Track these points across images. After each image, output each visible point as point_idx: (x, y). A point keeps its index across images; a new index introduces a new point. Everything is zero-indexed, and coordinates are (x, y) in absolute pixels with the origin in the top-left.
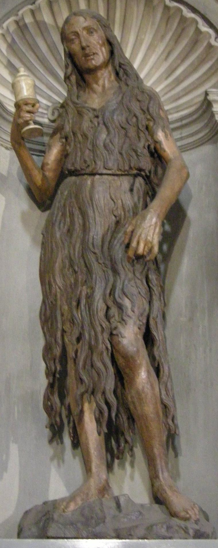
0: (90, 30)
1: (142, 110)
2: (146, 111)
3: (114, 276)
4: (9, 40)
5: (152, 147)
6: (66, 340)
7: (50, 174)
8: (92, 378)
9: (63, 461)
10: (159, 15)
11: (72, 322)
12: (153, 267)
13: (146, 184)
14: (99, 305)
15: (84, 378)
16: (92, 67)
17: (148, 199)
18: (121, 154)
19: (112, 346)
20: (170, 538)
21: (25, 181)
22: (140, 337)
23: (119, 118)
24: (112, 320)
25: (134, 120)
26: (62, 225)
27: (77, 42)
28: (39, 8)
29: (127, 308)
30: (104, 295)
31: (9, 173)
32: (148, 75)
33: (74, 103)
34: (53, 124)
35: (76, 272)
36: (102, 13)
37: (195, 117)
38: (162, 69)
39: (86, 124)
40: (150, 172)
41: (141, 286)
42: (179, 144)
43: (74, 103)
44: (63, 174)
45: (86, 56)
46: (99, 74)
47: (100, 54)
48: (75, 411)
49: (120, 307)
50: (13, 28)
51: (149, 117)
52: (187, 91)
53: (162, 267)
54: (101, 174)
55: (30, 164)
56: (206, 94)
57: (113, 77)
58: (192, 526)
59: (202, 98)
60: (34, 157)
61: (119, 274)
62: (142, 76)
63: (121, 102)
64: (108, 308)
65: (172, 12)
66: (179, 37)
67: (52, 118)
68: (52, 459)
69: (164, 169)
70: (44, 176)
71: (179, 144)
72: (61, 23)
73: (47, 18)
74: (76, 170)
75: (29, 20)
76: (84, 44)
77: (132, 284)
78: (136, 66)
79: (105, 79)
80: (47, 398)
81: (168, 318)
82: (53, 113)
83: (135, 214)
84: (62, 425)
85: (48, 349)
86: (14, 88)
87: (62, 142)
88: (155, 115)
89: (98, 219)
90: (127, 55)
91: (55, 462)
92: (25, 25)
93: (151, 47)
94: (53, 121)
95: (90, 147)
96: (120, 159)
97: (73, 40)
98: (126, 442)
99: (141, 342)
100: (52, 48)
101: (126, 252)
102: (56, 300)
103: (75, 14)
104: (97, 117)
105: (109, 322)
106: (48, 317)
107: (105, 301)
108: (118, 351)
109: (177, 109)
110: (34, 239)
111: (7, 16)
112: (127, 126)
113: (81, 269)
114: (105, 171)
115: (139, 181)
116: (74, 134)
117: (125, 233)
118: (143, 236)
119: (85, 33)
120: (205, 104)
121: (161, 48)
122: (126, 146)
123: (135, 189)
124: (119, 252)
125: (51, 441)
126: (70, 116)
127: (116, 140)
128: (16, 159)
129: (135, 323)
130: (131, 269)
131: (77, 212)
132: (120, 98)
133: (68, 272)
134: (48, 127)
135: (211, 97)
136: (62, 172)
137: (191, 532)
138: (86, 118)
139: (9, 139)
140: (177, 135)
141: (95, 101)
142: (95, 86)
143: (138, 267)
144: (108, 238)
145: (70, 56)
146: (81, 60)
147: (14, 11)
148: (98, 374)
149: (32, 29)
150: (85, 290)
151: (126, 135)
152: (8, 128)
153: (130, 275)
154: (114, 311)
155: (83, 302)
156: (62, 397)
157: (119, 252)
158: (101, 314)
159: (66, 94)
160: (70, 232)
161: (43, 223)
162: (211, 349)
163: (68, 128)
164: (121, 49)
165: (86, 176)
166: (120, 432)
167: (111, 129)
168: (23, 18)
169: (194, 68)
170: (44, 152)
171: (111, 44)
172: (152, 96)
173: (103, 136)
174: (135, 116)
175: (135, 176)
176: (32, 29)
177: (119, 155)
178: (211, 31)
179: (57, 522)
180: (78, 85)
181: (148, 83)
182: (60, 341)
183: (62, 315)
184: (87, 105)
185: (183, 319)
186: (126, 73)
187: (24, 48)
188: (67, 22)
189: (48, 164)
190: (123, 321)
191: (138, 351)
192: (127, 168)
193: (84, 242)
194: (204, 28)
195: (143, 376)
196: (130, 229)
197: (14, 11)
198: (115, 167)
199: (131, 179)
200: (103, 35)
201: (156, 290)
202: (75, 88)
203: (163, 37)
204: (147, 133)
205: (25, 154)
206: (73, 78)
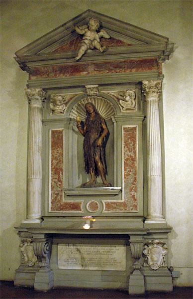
39: (90, 123)
44: (87, 132)
84: (88, 171)
85: (85, 160)
106: (85, 155)
113: (89, 148)
121: (104, 107)
145: (87, 111)
166: (97, 173)
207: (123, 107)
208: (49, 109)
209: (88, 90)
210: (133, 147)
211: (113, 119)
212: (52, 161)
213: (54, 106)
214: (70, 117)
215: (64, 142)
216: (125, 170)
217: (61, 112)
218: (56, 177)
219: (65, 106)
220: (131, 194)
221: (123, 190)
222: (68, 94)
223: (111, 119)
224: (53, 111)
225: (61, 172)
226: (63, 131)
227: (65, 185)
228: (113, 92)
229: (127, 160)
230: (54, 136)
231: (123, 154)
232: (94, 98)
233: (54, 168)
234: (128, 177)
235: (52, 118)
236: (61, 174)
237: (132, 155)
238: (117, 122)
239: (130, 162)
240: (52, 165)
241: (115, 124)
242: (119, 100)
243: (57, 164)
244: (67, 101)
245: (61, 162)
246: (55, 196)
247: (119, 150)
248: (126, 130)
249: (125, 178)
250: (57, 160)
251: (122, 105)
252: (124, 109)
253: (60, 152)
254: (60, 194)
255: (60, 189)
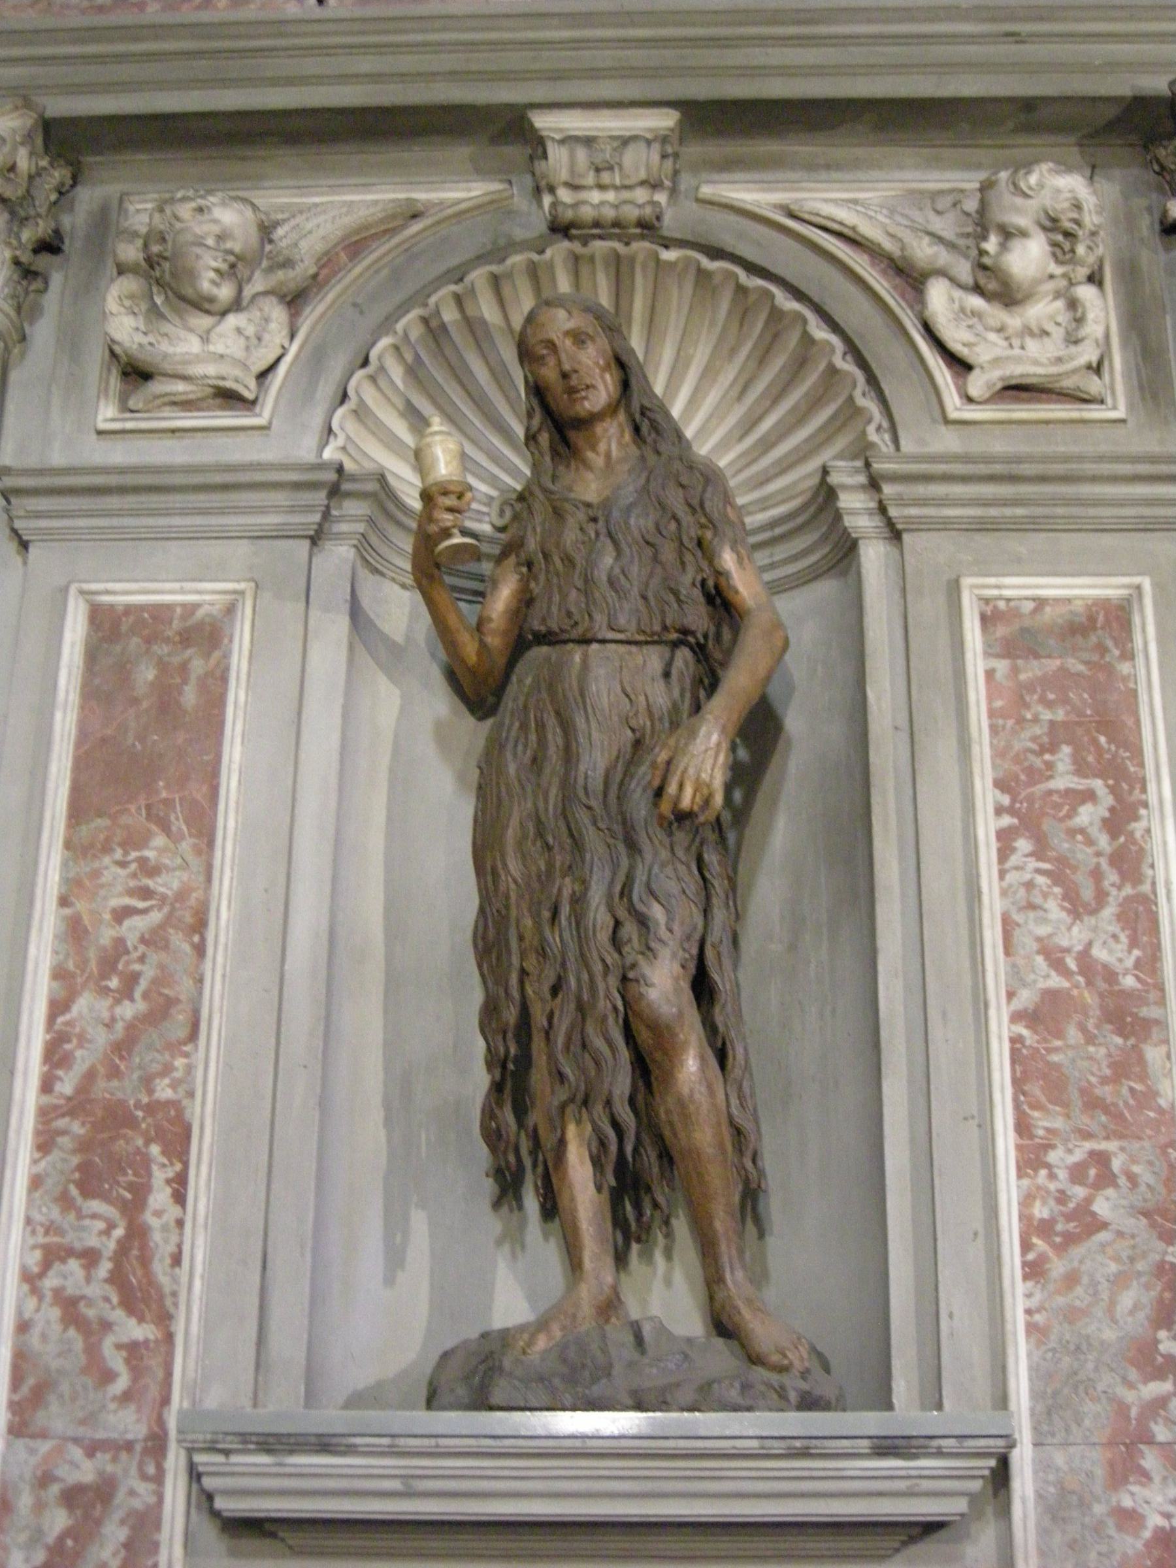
0: (579, 338)
1: (690, 505)
2: (697, 508)
3: (631, 856)
4: (409, 357)
5: (711, 583)
6: (529, 991)
7: (494, 641)
8: (583, 1071)
9: (523, 1246)
10: (725, 305)
11: (542, 952)
12: (712, 837)
13: (698, 661)
14: (599, 916)
15: (568, 1070)
16: (583, 414)
17: (702, 694)
18: (644, 598)
19: (626, 1004)
20: (749, 1409)
21: (442, 655)
22: (685, 986)
23: (641, 522)
24: (626, 949)
25: (673, 526)
26: (520, 748)
27: (551, 361)
28: (472, 291)
29: (657, 924)
30: (609, 896)
31: (408, 638)
32: (703, 431)
33: (545, 490)
34: (502, 536)
35: (549, 848)
36: (605, 300)
37: (800, 520)
38: (731, 420)
39: (571, 536)
40: (706, 636)
41: (687, 878)
42: (767, 577)
43: (545, 490)
44: (524, 639)
45: (572, 391)
46: (599, 429)
47: (601, 387)
48: (548, 1140)
49: (643, 922)
50: (416, 332)
51: (703, 520)
52: (784, 466)
53: (731, 837)
54: (603, 641)
55: (452, 620)
56: (825, 471)
57: (628, 436)
58: (794, 1385)
59: (815, 480)
60: (462, 605)
61: (640, 852)
62: (689, 433)
63: (645, 490)
64: (618, 924)
65: (752, 298)
66: (768, 350)
67: (500, 523)
68: (499, 1243)
69: (736, 631)
70: (483, 644)
71: (767, 577)
72: (517, 322)
73: (488, 310)
74: (550, 633)
75: (450, 315)
76: (567, 367)
77: (667, 876)
78: (676, 412)
79: (612, 440)
80: (489, 1114)
81: (743, 943)
82: (502, 513)
83: (675, 725)
84: (519, 1171)
85: (490, 1010)
86: (419, 460)
87: (521, 574)
88: (716, 516)
89: (595, 735)
90: (658, 389)
91: (506, 1248)
92: (443, 327)
93: (709, 374)
94: (502, 529)
95: (579, 583)
96: (642, 608)
97: (543, 357)
98: (656, 1205)
99: (688, 995)
100: (499, 374)
101: (656, 805)
102: (507, 907)
103: (548, 303)
104: (594, 520)
105: (620, 953)
106: (491, 943)
107: (611, 910)
108: (638, 1015)
109: (764, 504)
110: (461, 777)
111: (403, 308)
112: (657, 540)
114: (611, 635)
115: (684, 656)
116: (546, 556)
117: (654, 765)
118: (691, 771)
119: (568, 342)
120: (823, 493)
121: (729, 374)
122: (655, 582)
123: (674, 672)
124: (639, 807)
125: (497, 1205)
126: (538, 519)
127: (634, 570)
128: (423, 609)
129: (674, 955)
130: (667, 841)
131: (551, 722)
132: (642, 481)
133: (534, 848)
134: (492, 541)
135: (834, 479)
136: (520, 636)
137: (793, 1396)
138: (571, 522)
139: (408, 566)
140: (762, 557)
141: (589, 487)
142: (590, 455)
143: (681, 837)
144: (618, 777)
145: (538, 391)
146: (559, 399)
147: (420, 297)
148: (597, 1063)
149: (458, 336)
150: (568, 887)
151: (655, 559)
152: (407, 544)
153: (664, 854)
154: (630, 929)
155: (565, 910)
156: (521, 1111)
157: (639, 807)
158: (603, 936)
159: (528, 472)
160: (536, 762)
161: (481, 743)
162: (834, 1011)
163: (532, 544)
164: (645, 377)
165: (570, 646)
166: (644, 1182)
167: (624, 545)
168: (438, 312)
169: (799, 417)
170: (482, 594)
171: (623, 367)
172: (710, 477)
173: (608, 560)
174: (675, 517)
175: (675, 645)
176: (458, 336)
177: (640, 602)
178: (834, 339)
179: (510, 1374)
180: (555, 454)
181: (703, 450)
182: (516, 994)
183: (521, 938)
184: (572, 495)
185: (776, 947)
186: (655, 427)
187: (440, 375)
188: (530, 319)
189: (490, 620)
190: (648, 951)
191: (680, 1014)
192: (657, 628)
193: (566, 784)
194: (820, 333)
195: (691, 1067)
196: (663, 757)
197: (420, 297)
198: (633, 626)
199: (666, 650)
200: (608, 347)
201: (719, 886)
202: (548, 459)
203: (733, 351)
204: (699, 554)
205: (443, 598)
206: (544, 438)
207: (960, 365)
208: (96, 356)
209: (558, 159)
210: (1103, 841)
211: (854, 504)
212: (57, 1007)
213: (155, 313)
214: (328, 454)
215: (233, 753)
216: (1032, 1159)
217: (228, 397)
218: (93, 1241)
219: (278, 314)
220: (1129, 1519)
221: (1023, 1460)
222: (323, 207)
223: (826, 494)
224: (136, 373)
225: (160, 1176)
226: (230, 610)
227: (205, 1370)
228: (864, 198)
229: (1044, 1015)
230: (123, 671)
231: (992, 936)
232: (620, 268)
233: (77, 1106)
234: (1077, 1251)
235: (118, 454)
236: (160, 1197)
237: (1113, 952)
238: (895, 534)
239: (1083, 1054)
240: (56, 1055)
241: (874, 556)
242: (911, 278)
243: (123, 1047)
244: (306, 267)
245: (170, 1017)
246: (58, 1520)
247: (940, 882)
248: (1015, 633)
249: (1034, 1270)
250: (127, 992)
251: (956, 337)
252: (977, 384)
253: (167, 884)
254: (134, 1491)
255: (129, 1423)
